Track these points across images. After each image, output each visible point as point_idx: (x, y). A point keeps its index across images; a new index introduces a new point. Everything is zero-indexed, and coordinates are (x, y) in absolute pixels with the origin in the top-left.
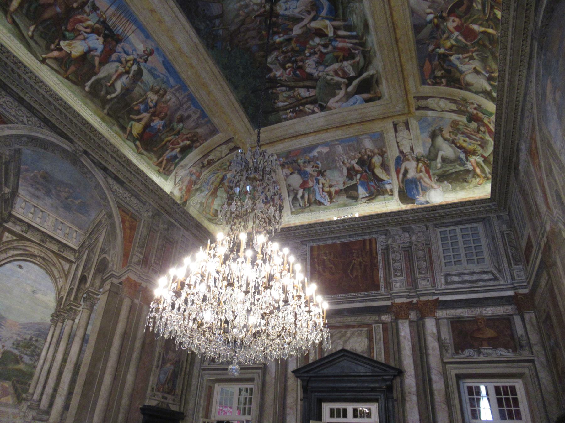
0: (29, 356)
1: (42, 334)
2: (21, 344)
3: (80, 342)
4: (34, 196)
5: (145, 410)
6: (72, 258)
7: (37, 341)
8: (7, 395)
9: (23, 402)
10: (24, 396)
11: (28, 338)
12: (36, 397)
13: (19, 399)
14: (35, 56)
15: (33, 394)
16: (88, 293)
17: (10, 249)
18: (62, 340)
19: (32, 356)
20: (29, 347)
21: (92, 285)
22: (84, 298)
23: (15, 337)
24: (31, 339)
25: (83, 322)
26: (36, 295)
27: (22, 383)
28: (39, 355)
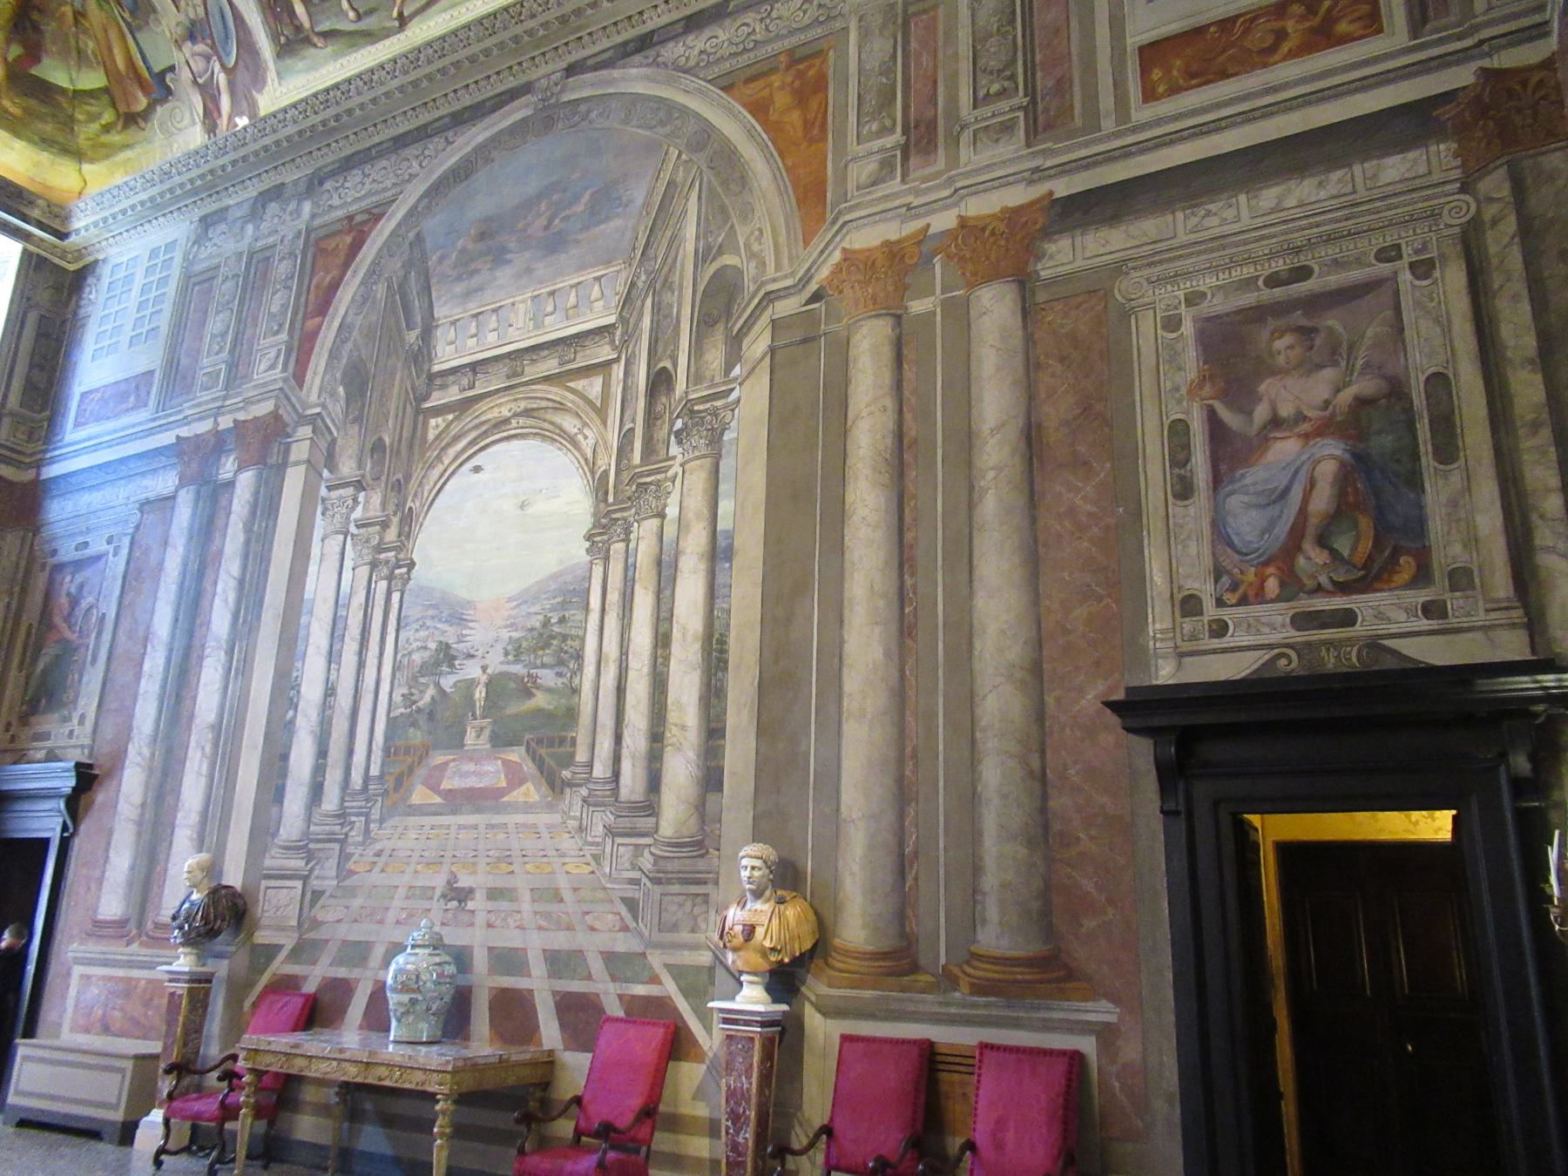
0: (551, 667)
1: (573, 595)
2: (524, 644)
3: (702, 566)
4: (468, 295)
5: (1139, 709)
6: (605, 353)
7: (562, 620)
8: (522, 782)
9: (568, 791)
10: (566, 774)
11: (538, 625)
12: (600, 770)
13: (556, 786)
14: (387, 34)
15: (590, 765)
16: (689, 411)
17: (448, 445)
18: (637, 587)
19: (561, 663)
20: (547, 645)
21: (695, 377)
22: (678, 434)
23: (505, 634)
24: (546, 623)
25: (697, 501)
26: (530, 510)
27: (551, 744)
28: (579, 657)
